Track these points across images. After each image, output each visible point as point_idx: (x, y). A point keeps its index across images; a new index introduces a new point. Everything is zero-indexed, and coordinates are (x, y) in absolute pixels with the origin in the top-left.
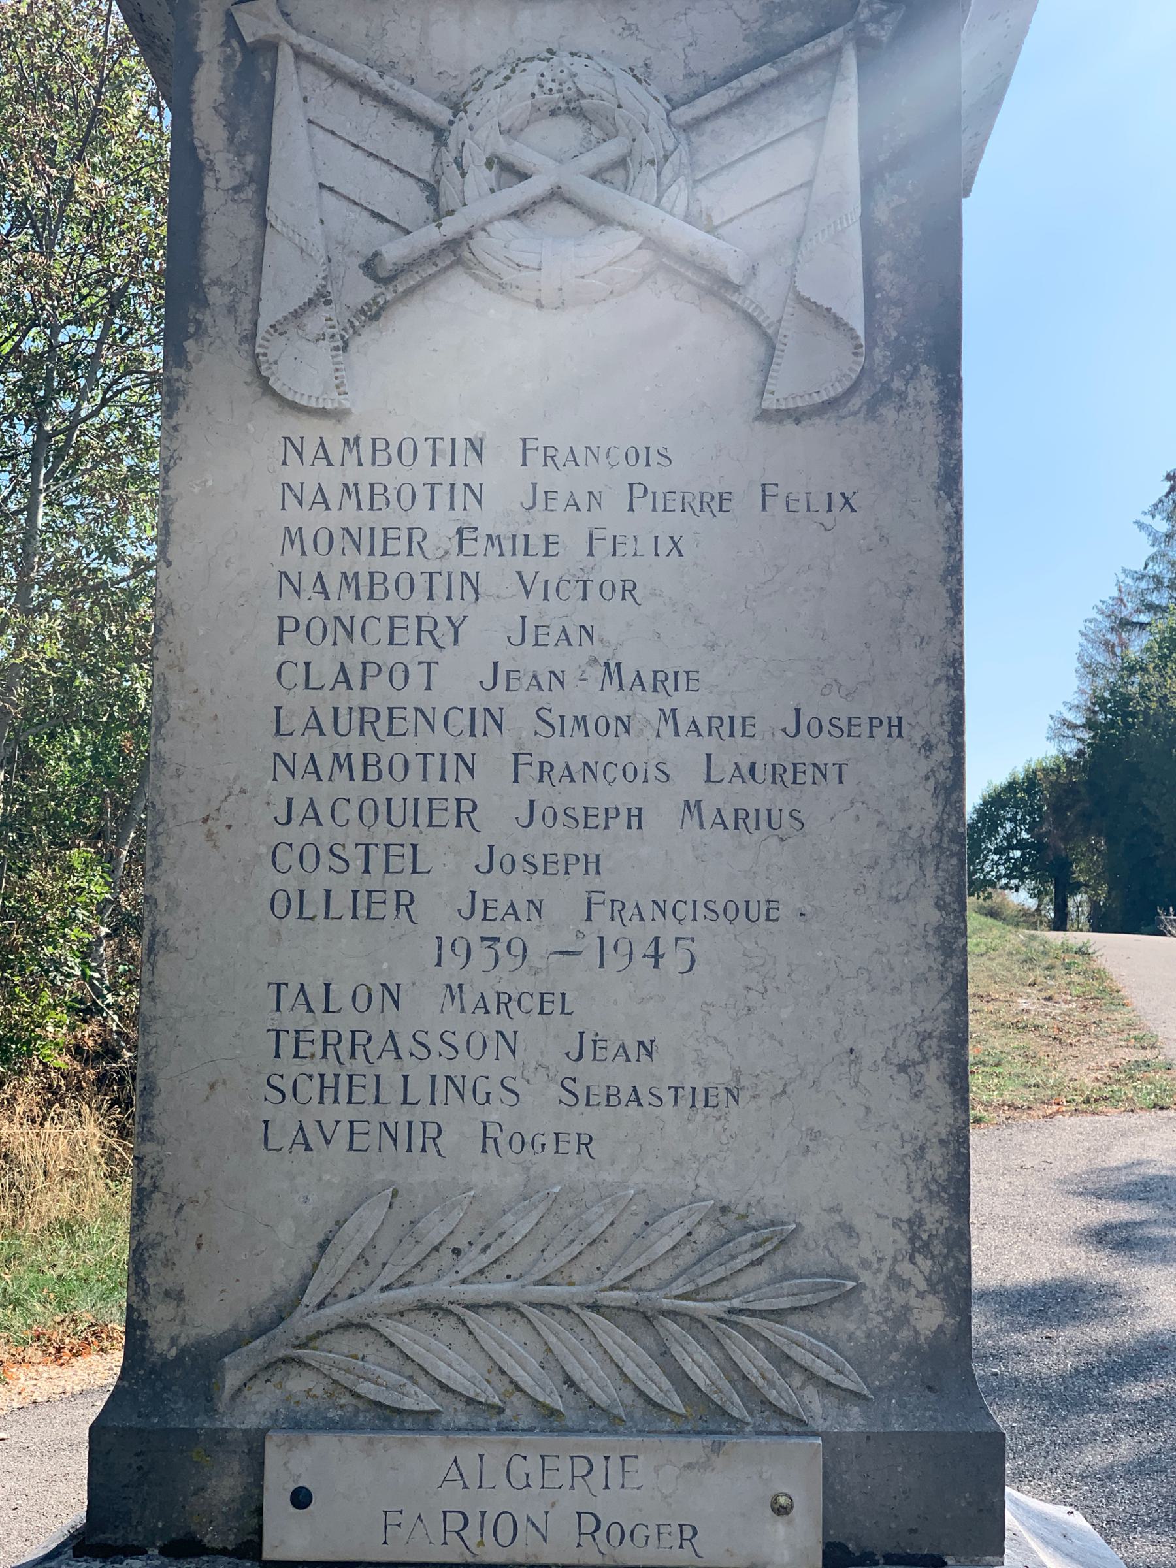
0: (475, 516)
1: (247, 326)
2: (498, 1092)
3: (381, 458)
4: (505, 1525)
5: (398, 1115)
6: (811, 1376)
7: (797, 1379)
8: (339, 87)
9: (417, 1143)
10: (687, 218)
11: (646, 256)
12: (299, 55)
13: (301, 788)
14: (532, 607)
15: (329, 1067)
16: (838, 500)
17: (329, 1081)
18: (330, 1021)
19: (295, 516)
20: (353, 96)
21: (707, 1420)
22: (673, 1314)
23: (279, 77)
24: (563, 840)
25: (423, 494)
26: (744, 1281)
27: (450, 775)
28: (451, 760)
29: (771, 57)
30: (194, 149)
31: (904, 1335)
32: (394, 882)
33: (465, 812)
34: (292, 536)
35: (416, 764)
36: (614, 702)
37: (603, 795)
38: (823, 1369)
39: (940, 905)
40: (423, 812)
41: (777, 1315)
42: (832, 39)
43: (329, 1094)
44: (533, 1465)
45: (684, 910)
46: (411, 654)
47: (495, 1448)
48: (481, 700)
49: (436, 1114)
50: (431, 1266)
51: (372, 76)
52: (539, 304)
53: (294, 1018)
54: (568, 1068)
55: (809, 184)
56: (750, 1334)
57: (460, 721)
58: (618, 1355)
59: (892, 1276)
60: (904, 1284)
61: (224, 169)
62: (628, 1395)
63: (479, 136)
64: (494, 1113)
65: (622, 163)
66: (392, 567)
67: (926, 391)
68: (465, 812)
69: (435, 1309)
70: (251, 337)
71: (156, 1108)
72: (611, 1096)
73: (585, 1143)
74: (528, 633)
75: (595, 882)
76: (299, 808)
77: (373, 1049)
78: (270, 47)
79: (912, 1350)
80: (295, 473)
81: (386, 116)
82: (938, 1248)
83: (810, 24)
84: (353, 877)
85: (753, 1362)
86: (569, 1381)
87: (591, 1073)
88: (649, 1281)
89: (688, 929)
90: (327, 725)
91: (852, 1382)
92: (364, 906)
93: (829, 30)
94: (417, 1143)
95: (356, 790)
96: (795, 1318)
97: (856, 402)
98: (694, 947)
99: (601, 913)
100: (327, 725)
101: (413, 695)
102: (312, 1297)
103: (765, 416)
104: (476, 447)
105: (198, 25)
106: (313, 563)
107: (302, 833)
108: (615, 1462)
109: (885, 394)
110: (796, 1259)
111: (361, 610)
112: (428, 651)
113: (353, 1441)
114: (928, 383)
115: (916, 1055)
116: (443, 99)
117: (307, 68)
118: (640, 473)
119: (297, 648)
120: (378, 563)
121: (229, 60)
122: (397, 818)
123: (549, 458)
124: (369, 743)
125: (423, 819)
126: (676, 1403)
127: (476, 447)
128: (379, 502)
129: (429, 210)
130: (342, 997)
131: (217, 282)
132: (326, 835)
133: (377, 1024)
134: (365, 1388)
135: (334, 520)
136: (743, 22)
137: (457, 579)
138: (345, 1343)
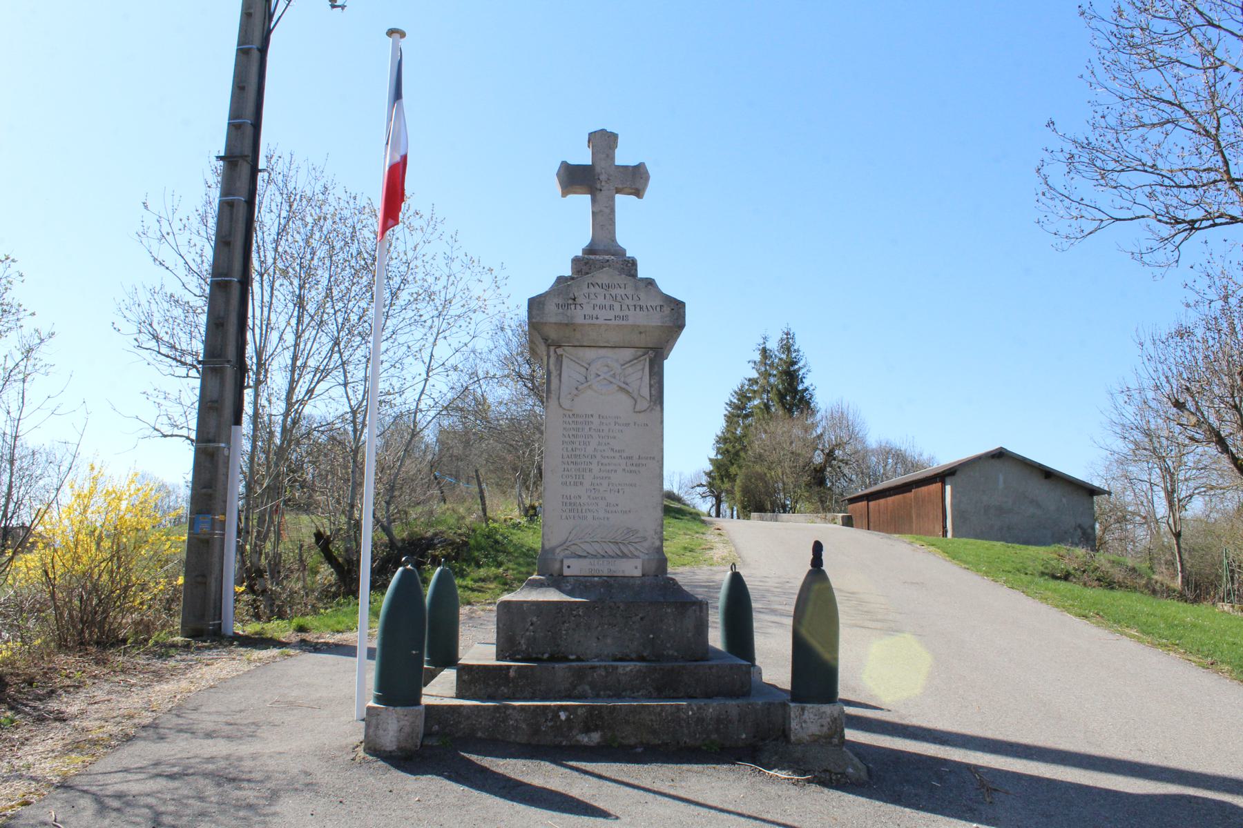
21: (624, 556)
33: (590, 470)
36: (612, 454)
63: (593, 369)
67: (658, 408)
85: (632, 549)
92: (575, 484)
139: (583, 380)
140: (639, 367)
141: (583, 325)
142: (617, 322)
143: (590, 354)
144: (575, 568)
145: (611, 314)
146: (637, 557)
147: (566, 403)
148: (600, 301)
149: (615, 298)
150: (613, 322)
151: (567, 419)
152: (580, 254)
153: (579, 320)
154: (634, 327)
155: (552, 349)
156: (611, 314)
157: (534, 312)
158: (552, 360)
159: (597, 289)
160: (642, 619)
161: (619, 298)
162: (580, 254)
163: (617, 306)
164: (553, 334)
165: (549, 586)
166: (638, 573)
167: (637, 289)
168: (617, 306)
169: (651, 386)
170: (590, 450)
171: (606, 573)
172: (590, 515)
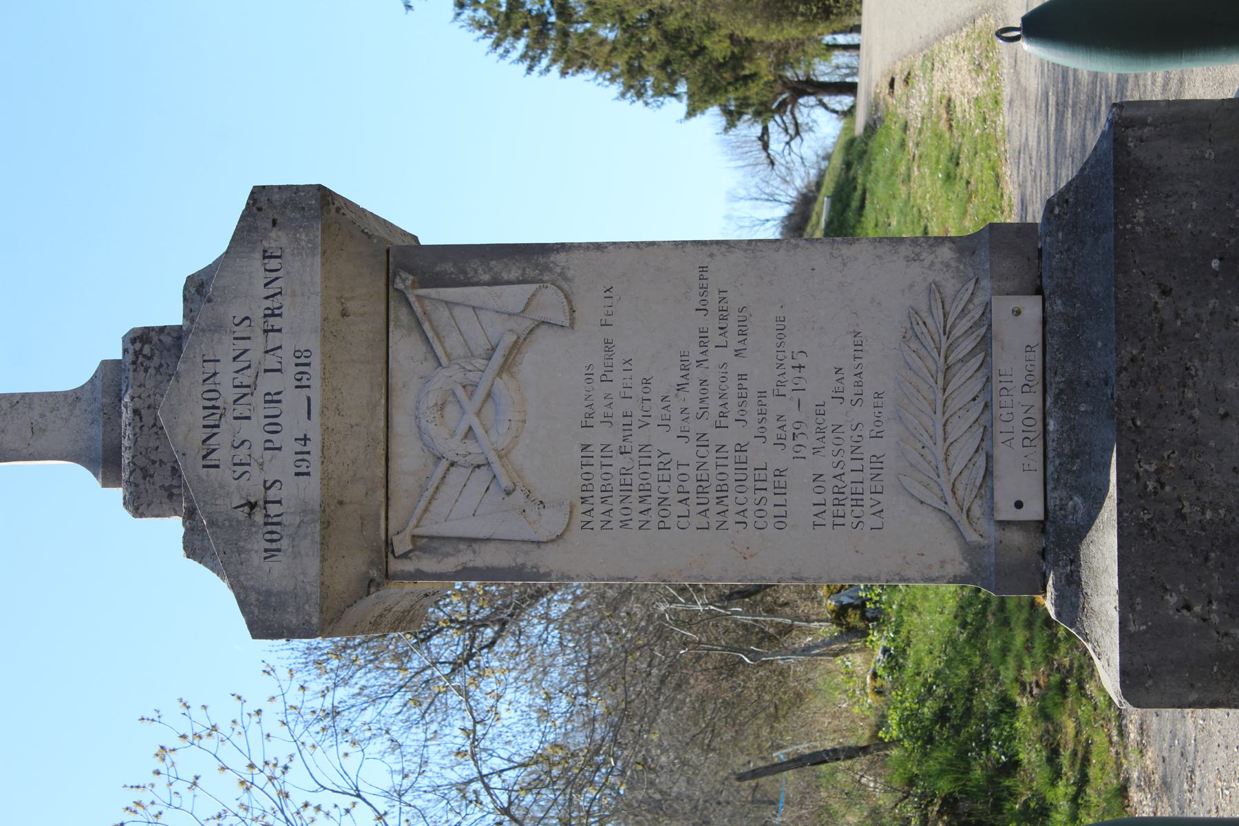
0: (615, 447)
1: (534, 546)
2: (858, 432)
3: (590, 487)
4: (1027, 422)
5: (868, 473)
6: (970, 301)
7: (971, 306)
8: (431, 508)
9: (879, 465)
10: (490, 359)
11: (505, 376)
12: (417, 526)
13: (731, 518)
14: (653, 422)
15: (848, 503)
16: (608, 294)
17: (854, 503)
18: (829, 503)
19: (615, 524)
20: (435, 503)
21: (985, 343)
22: (946, 358)
23: (427, 534)
24: (752, 407)
25: (605, 469)
26: (933, 329)
27: (725, 455)
28: (719, 455)
29: (419, 324)
30: (457, 572)
31: (953, 264)
32: (771, 478)
33: (741, 449)
34: (624, 524)
35: (721, 469)
36: (694, 387)
37: (733, 391)
38: (967, 296)
39: (777, 250)
40: (741, 466)
41: (945, 315)
42: (412, 299)
43: (860, 503)
44: (1004, 411)
45: (781, 356)
46: (674, 473)
47: (999, 426)
48: (694, 443)
49: (867, 457)
50: (930, 457)
51: (428, 494)
52: (524, 421)
53: (828, 519)
54: (847, 402)
55: (474, 308)
56: (953, 326)
57: (702, 451)
58: (963, 379)
59: (929, 269)
60: (932, 264)
61: (466, 558)
62: (979, 374)
63: (452, 447)
64: (866, 433)
65: (464, 387)
66: (637, 482)
67: (561, 258)
68: (741, 449)
69: (947, 455)
70: (539, 543)
71: (866, 575)
72: (858, 385)
73: (878, 395)
74: (665, 424)
75: (769, 393)
76: (740, 518)
77: (841, 484)
78: (414, 537)
79: (959, 260)
80: (597, 524)
81: (443, 488)
82: (918, 250)
84: (769, 494)
85: (964, 325)
86: (974, 399)
87: (849, 394)
88: (933, 368)
89: (789, 354)
90: (705, 507)
91: (971, 285)
92: (780, 490)
93: (407, 300)
94: (879, 465)
95: (732, 494)
96: (947, 308)
97: (565, 286)
98: (796, 351)
99: (782, 390)
100: (705, 507)
101: (691, 471)
102: (941, 506)
103: (572, 326)
104: (585, 447)
106: (635, 516)
107: (750, 517)
108: (1002, 379)
109: (562, 274)
110: (923, 307)
111: (655, 494)
112: (673, 466)
113: (997, 485)
114: (558, 257)
115: (840, 259)
116: (436, 465)
117: (423, 522)
118: (596, 378)
119: (672, 521)
120: (635, 487)
121: (418, 557)
122: (743, 477)
123: (590, 416)
124: (712, 490)
125: (744, 466)
126: (981, 356)
127: (585, 447)
128: (609, 488)
129: (484, 469)
130: (819, 499)
131: (514, 560)
132: (751, 507)
133: (830, 483)
134: (978, 484)
135: (617, 507)
137: (642, 454)
138: (960, 493)
139: (482, 476)
140: (442, 314)
141: (326, 478)
142: (316, 382)
143: (409, 458)
144: (1021, 488)
145: (293, 401)
146: (988, 306)
147: (551, 522)
148: (254, 431)
150: (316, 394)
151: (597, 518)
152: (117, 494)
153: (312, 489)
154: (328, 333)
155: (396, 566)
156: (293, 401)
157: (292, 619)
158: (428, 564)
159: (223, 439)
160: (1165, 292)
161: (245, 378)
162: (117, 494)
163: (268, 383)
164: (353, 565)
165: (1075, 561)
166: (1032, 307)
167: (217, 327)
168: (268, 383)
169: (495, 282)
170: (685, 452)
171: (1036, 399)
172: (870, 448)
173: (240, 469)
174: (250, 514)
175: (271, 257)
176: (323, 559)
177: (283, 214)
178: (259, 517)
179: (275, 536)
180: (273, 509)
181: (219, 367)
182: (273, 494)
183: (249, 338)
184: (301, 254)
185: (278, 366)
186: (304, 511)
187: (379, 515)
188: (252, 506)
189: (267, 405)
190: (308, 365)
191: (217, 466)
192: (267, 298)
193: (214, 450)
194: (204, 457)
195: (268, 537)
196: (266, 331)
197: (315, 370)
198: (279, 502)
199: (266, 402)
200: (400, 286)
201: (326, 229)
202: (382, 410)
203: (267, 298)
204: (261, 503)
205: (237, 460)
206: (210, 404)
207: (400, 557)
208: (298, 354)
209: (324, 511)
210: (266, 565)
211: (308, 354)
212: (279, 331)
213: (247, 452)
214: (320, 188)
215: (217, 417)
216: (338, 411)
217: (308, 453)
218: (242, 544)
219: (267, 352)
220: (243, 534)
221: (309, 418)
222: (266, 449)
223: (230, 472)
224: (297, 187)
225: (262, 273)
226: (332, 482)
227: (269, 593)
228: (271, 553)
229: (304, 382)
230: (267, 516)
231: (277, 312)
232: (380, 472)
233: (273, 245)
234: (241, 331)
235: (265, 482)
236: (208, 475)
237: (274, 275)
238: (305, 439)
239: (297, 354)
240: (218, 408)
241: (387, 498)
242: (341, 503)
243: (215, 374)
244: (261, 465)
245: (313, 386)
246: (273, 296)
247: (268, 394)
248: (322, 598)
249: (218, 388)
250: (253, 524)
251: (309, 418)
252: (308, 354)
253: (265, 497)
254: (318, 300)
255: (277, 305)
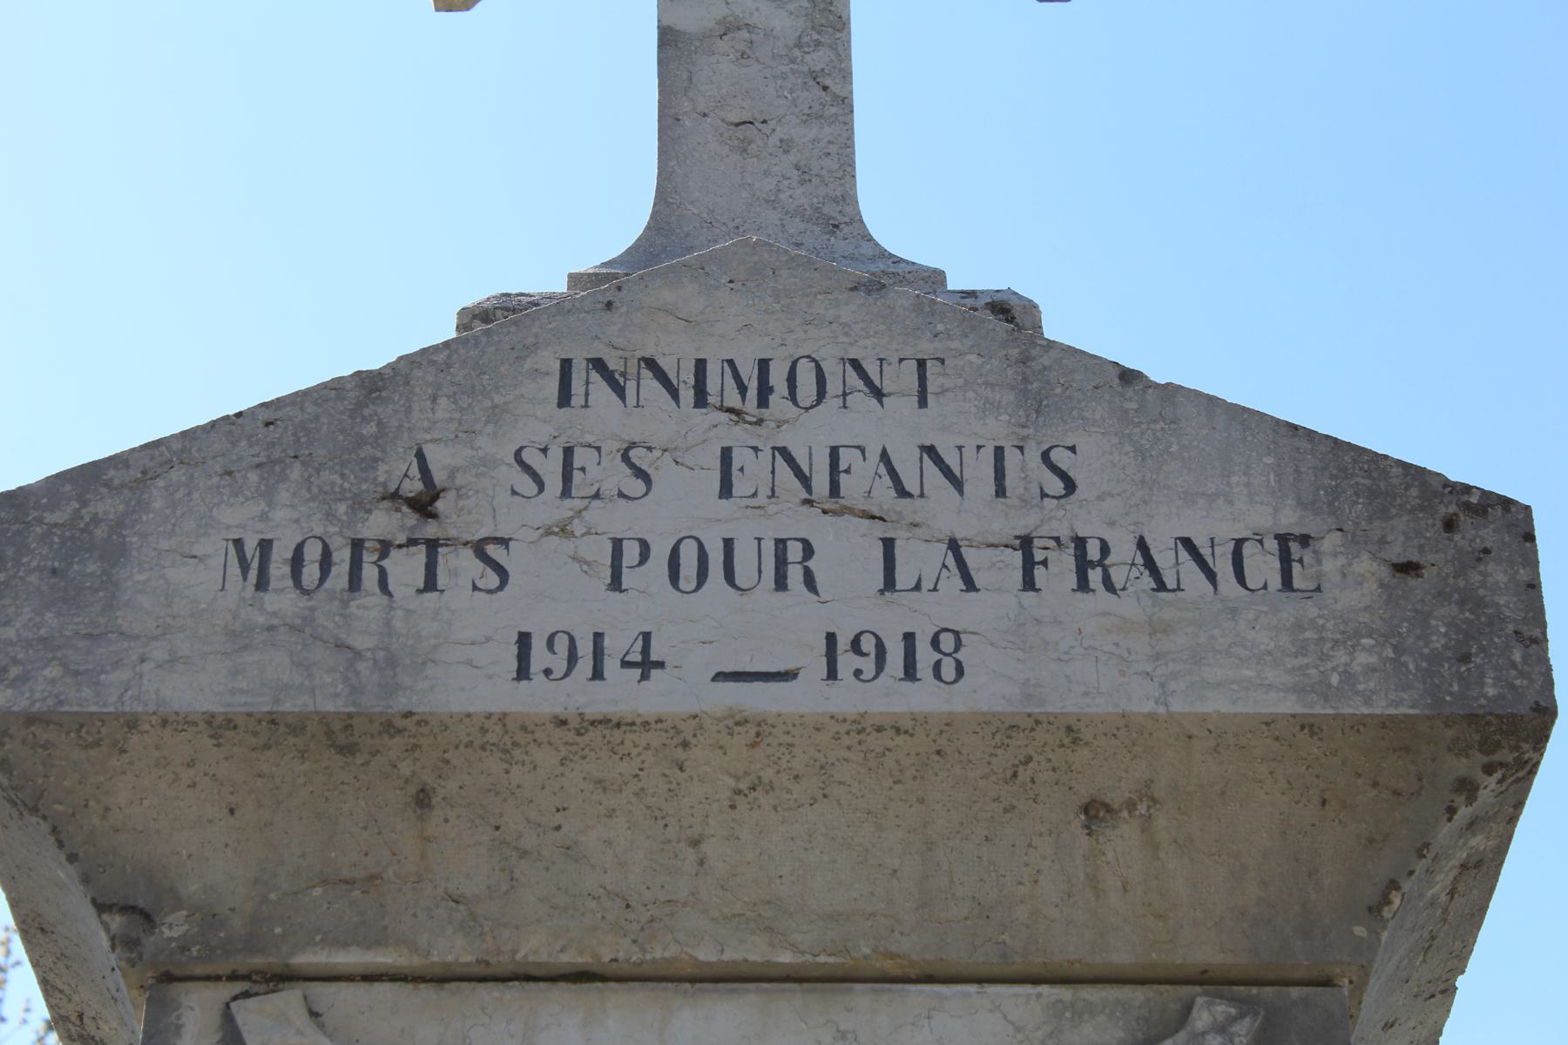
83: (1121, 1034)
105: (178, 1030)
136: (1019, 1029)
141: (504, 736)
142: (847, 698)
145: (786, 627)
148: (682, 505)
149: (827, 488)
150: (808, 697)
153: (468, 680)
154: (1029, 743)
156: (786, 627)
159: (654, 416)
161: (861, 480)
163: (846, 553)
164: (207, 852)
168: (846, 553)
173: (550, 469)
174: (395, 496)
175: (1286, 559)
176: (219, 726)
177: (1442, 596)
178: (381, 523)
179: (311, 572)
180: (406, 568)
181: (902, 406)
182: (460, 566)
183: (1001, 491)
184: (1302, 650)
185: (904, 578)
186: (392, 662)
187: (378, 943)
188: (424, 506)
189: (769, 548)
190: (910, 672)
191: (564, 399)
192: (1142, 545)
193: (620, 392)
194: (598, 364)
195: (313, 552)
196: (1026, 543)
197: (890, 697)
198: (430, 584)
199: (781, 544)
200: (1202, 1018)
201: (1395, 734)
202: (752, 951)
203: (1142, 545)
204: (431, 530)
205: (581, 457)
206: (778, 378)
207: (228, 1018)
208: (947, 642)
209: (389, 728)
210: (214, 547)
211: (948, 671)
212: (1029, 584)
213: (609, 488)
214: (1545, 714)
215: (733, 399)
216: (749, 789)
217: (598, 674)
218: (296, 472)
219: (954, 545)
220: (330, 477)
221: (721, 676)
222: (617, 544)
223: (542, 437)
224: (1540, 641)
225: (1228, 531)
226: (493, 763)
227: (115, 554)
228: (256, 562)
229: (847, 662)
230: (385, 547)
231: (1095, 576)
232: (535, 948)
233: (1329, 565)
234: (1025, 469)
235: (504, 542)
236: (536, 373)
237: (1224, 568)
238: (647, 665)
239: (949, 640)
240: (763, 402)
241: (442, 978)
242: (423, 799)
243: (878, 394)
244: (564, 530)
245: (834, 689)
246: (1150, 564)
247: (808, 551)
248: (81, 722)
249: (831, 403)
250: (360, 506)
251: (721, 676)
252: (948, 671)
253: (450, 542)
254: (1141, 700)
255: (1118, 576)
